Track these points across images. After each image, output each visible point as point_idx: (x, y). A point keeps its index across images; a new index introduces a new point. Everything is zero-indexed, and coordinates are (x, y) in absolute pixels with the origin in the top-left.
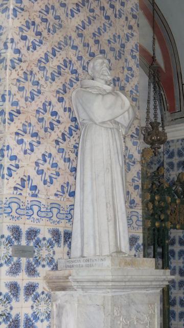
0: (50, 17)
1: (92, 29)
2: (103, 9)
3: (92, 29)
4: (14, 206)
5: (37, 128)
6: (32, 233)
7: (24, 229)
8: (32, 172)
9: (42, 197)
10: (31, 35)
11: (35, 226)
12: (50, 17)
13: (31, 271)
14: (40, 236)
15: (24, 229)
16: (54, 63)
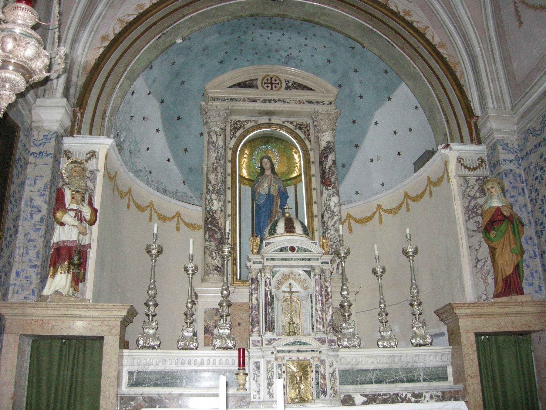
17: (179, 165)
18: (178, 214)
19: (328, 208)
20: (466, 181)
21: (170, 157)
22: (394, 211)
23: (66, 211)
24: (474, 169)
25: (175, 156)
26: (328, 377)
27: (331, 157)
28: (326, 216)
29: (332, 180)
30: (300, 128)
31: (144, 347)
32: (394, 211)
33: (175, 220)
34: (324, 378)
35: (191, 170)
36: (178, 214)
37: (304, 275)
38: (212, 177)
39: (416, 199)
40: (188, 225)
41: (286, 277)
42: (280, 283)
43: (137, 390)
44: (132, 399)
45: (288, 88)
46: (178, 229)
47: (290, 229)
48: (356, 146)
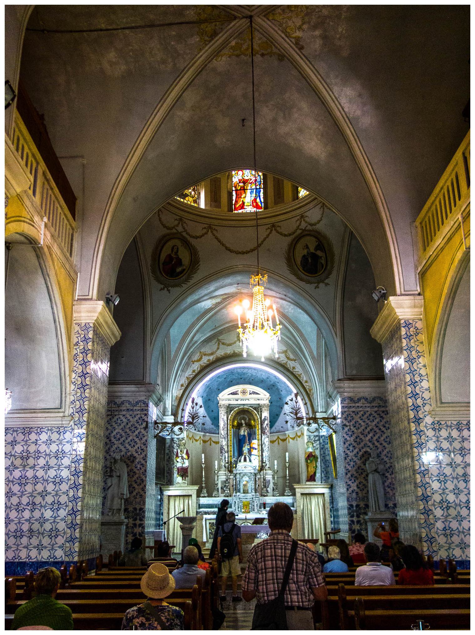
0: (358, 440)
1: (375, 438)
2: (380, 429)
3: (375, 438)
4: (350, 499)
5: (356, 475)
6: (357, 506)
7: (354, 505)
8: (356, 488)
9: (360, 495)
10: (351, 448)
11: (359, 503)
12: (358, 440)
13: (358, 516)
14: (361, 506)
15: (354, 505)
16: (361, 453)
17: (210, 417)
18: (210, 439)
19: (264, 443)
20: (310, 437)
21: (206, 415)
22: (293, 439)
23: (179, 457)
24: (313, 433)
25: (208, 414)
26: (255, 505)
27: (266, 422)
28: (263, 446)
29: (266, 431)
30: (255, 409)
31: (203, 497)
32: (293, 439)
33: (209, 442)
34: (254, 506)
35: (215, 418)
36: (210, 439)
37: (249, 474)
38: (222, 432)
39: (299, 437)
40: (214, 442)
41: (244, 475)
42: (242, 477)
43: (201, 510)
44: (200, 512)
45: (250, 394)
46: (210, 445)
47: (245, 460)
48: (282, 408)
